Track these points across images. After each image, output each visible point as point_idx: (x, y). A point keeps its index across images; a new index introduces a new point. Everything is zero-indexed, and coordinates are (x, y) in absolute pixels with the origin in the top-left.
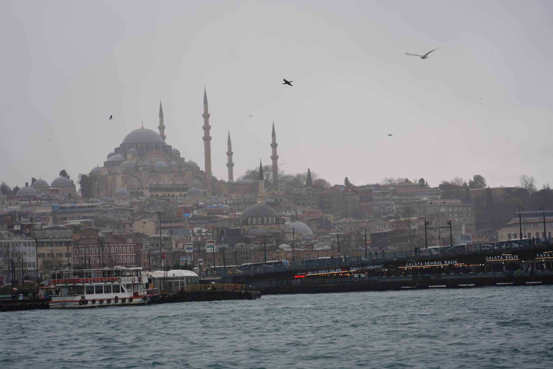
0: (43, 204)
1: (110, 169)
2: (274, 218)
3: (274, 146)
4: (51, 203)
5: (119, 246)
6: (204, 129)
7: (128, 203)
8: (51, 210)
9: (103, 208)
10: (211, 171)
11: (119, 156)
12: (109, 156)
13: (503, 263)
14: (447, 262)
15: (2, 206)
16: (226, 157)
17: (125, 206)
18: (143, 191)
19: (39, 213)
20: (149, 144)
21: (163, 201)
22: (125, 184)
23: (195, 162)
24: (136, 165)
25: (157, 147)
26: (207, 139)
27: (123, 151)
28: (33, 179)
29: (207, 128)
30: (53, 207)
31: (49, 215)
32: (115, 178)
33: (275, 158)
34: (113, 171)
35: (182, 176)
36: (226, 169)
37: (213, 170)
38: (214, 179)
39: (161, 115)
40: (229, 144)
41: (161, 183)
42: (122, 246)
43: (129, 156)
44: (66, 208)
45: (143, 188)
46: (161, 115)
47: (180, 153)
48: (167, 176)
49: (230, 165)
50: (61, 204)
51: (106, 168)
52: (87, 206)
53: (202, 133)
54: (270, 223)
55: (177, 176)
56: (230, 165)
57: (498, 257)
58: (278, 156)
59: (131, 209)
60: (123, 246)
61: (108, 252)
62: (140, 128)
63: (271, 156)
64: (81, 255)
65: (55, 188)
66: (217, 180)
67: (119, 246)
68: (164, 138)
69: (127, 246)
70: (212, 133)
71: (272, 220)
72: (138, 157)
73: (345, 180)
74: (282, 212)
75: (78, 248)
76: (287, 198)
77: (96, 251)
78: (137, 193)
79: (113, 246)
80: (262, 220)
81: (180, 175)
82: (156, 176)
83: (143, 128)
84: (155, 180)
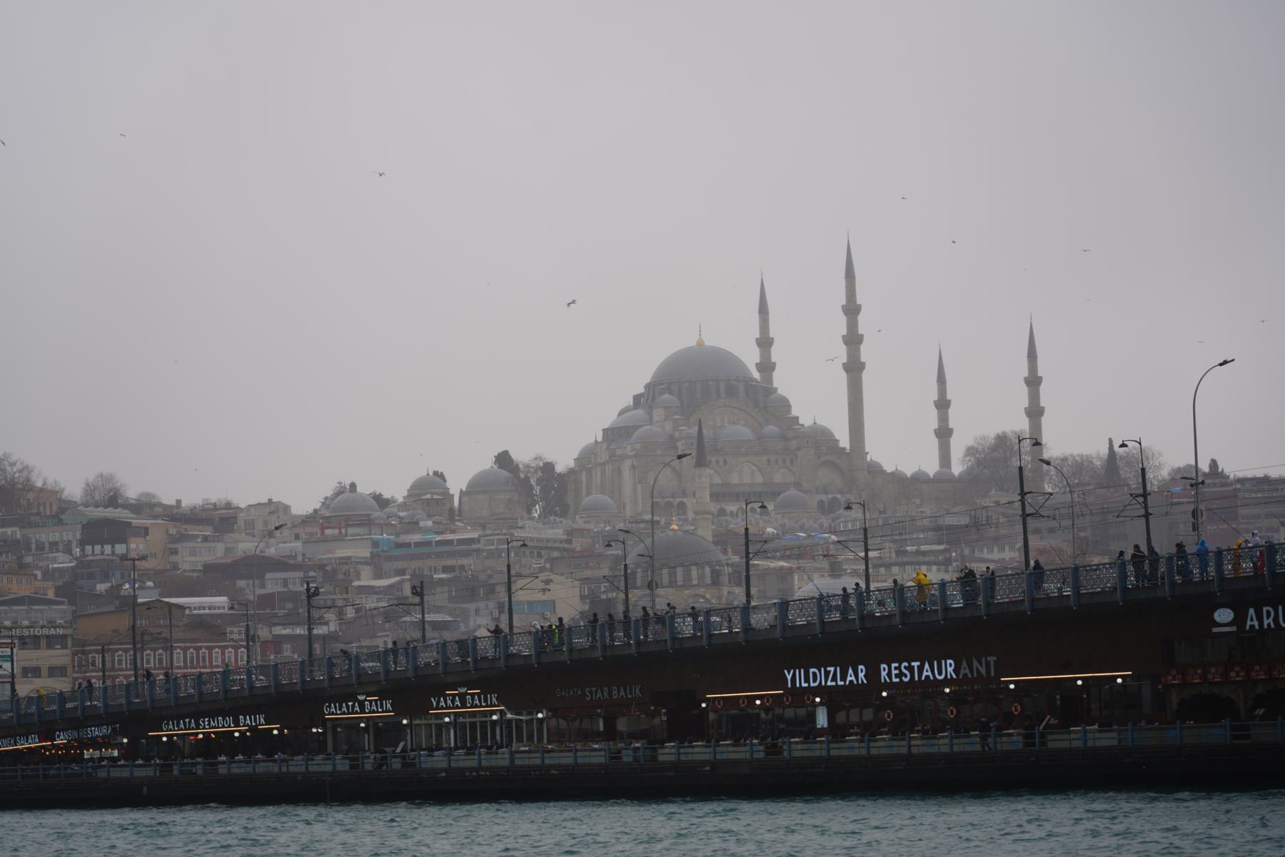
0: (352, 535)
1: (613, 446)
2: (708, 570)
3: (1033, 382)
4: (370, 534)
5: (201, 648)
6: (846, 343)
7: (561, 531)
8: (370, 550)
9: (485, 545)
10: (863, 448)
11: (640, 412)
12: (621, 413)
13: (362, 725)
14: (245, 719)
15: (267, 542)
16: (934, 413)
17: (548, 541)
18: (685, 500)
19: (336, 559)
20: (710, 383)
21: (642, 525)
22: (639, 483)
23: (825, 425)
24: (671, 437)
25: (731, 391)
26: (854, 368)
27: (649, 401)
28: (434, 472)
29: (853, 340)
30: (376, 544)
31: (360, 563)
32: (619, 470)
33: (1035, 412)
34: (618, 452)
35: (788, 461)
36: (934, 442)
37: (869, 447)
38: (876, 469)
39: (763, 310)
41: (735, 480)
42: (210, 649)
43: (658, 414)
44: (408, 545)
45: (684, 494)
46: (763, 310)
47: (791, 403)
48: (748, 462)
49: (944, 433)
50: (398, 535)
51: (605, 446)
52: (457, 539)
53: (842, 353)
54: (695, 582)
55: (777, 462)
56: (944, 433)
57: (350, 704)
58: (1043, 408)
59: (566, 546)
60: (214, 648)
61: (164, 664)
62: (692, 343)
63: (1025, 408)
64: (92, 671)
65: (435, 497)
66: (882, 472)
67: (201, 648)
68: (766, 367)
69: (226, 647)
70: (866, 353)
71: (701, 577)
72: (677, 417)
73: (1210, 465)
74: (982, 551)
75: (84, 652)
76: (1004, 515)
77: (161, 660)
78: (669, 505)
79: (181, 648)
80: (672, 575)
81: (784, 461)
82: (721, 463)
83: (700, 344)
84: (717, 472)
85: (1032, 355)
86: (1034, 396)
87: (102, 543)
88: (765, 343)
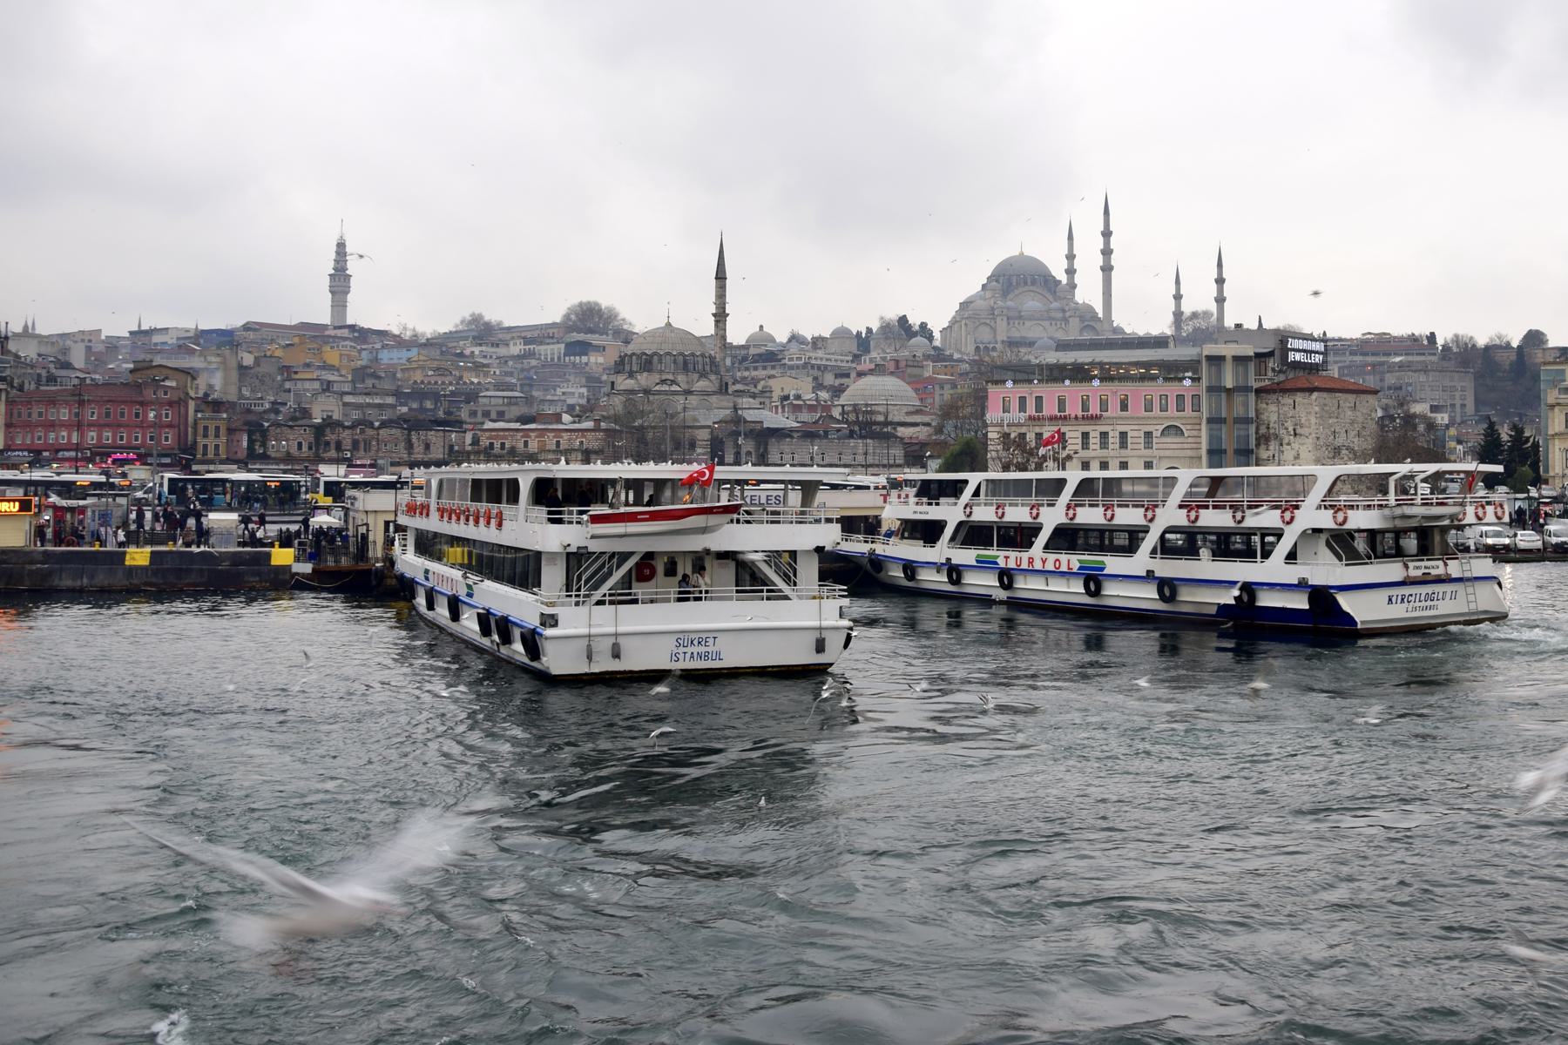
3: (1220, 281)
26: (1107, 269)
29: (1107, 252)
33: (1220, 300)
39: (1070, 237)
40: (1178, 282)
46: (1070, 237)
53: (1100, 260)
56: (1178, 314)
68: (1071, 272)
70: (1115, 260)
83: (1022, 254)
85: (1220, 265)
86: (1220, 290)
87: (575, 355)
88: (1071, 257)
